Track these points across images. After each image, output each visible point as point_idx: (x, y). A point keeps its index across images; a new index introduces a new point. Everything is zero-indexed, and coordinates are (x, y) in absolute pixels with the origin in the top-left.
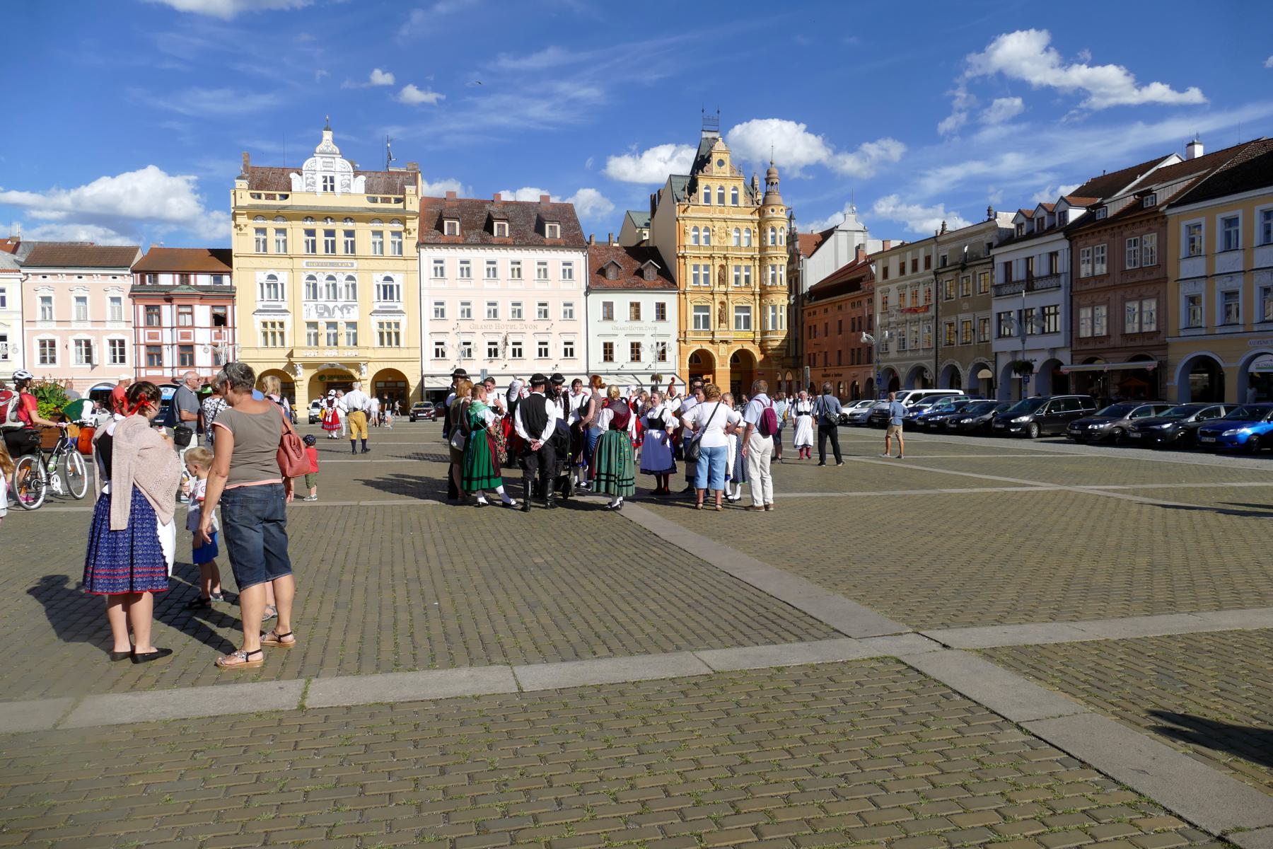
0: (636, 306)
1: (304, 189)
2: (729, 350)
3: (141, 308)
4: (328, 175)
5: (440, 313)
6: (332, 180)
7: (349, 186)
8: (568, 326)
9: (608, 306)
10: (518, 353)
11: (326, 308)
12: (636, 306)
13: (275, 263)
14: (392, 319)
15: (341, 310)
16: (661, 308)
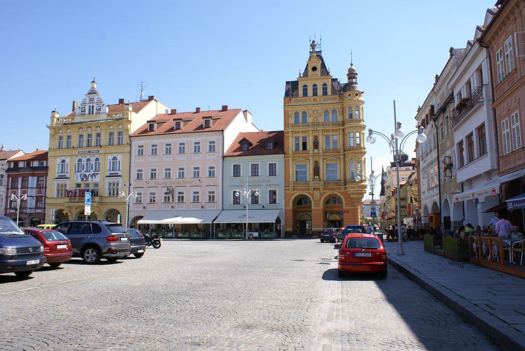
0: (255, 168)
1: (80, 113)
2: (321, 195)
3: (11, 179)
4: (91, 105)
5: (139, 176)
6: (93, 106)
7: (100, 110)
8: (211, 181)
9: (237, 169)
10: (181, 199)
11: (85, 175)
12: (255, 168)
13: (66, 152)
14: (115, 180)
15: (92, 176)
16: (272, 168)
